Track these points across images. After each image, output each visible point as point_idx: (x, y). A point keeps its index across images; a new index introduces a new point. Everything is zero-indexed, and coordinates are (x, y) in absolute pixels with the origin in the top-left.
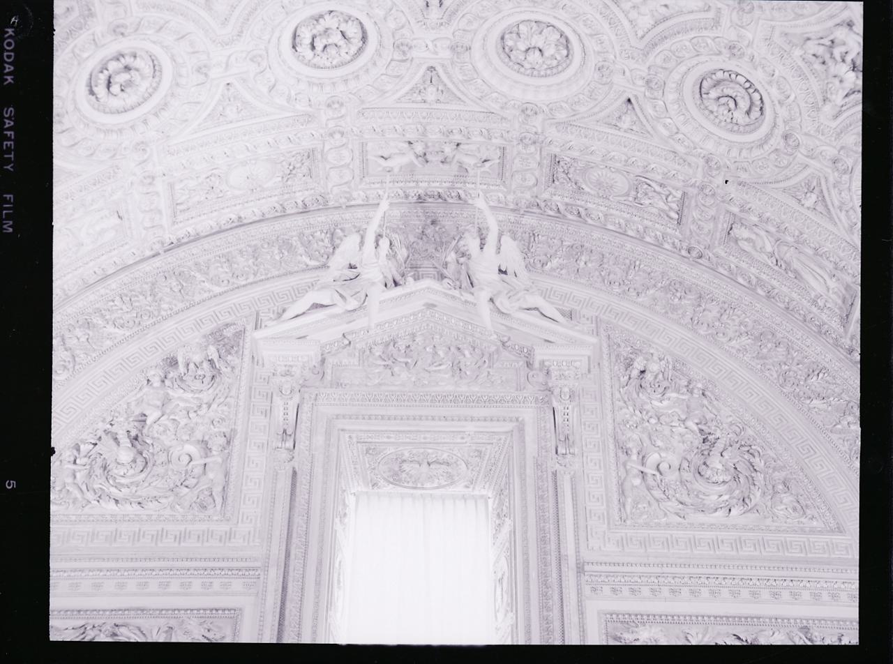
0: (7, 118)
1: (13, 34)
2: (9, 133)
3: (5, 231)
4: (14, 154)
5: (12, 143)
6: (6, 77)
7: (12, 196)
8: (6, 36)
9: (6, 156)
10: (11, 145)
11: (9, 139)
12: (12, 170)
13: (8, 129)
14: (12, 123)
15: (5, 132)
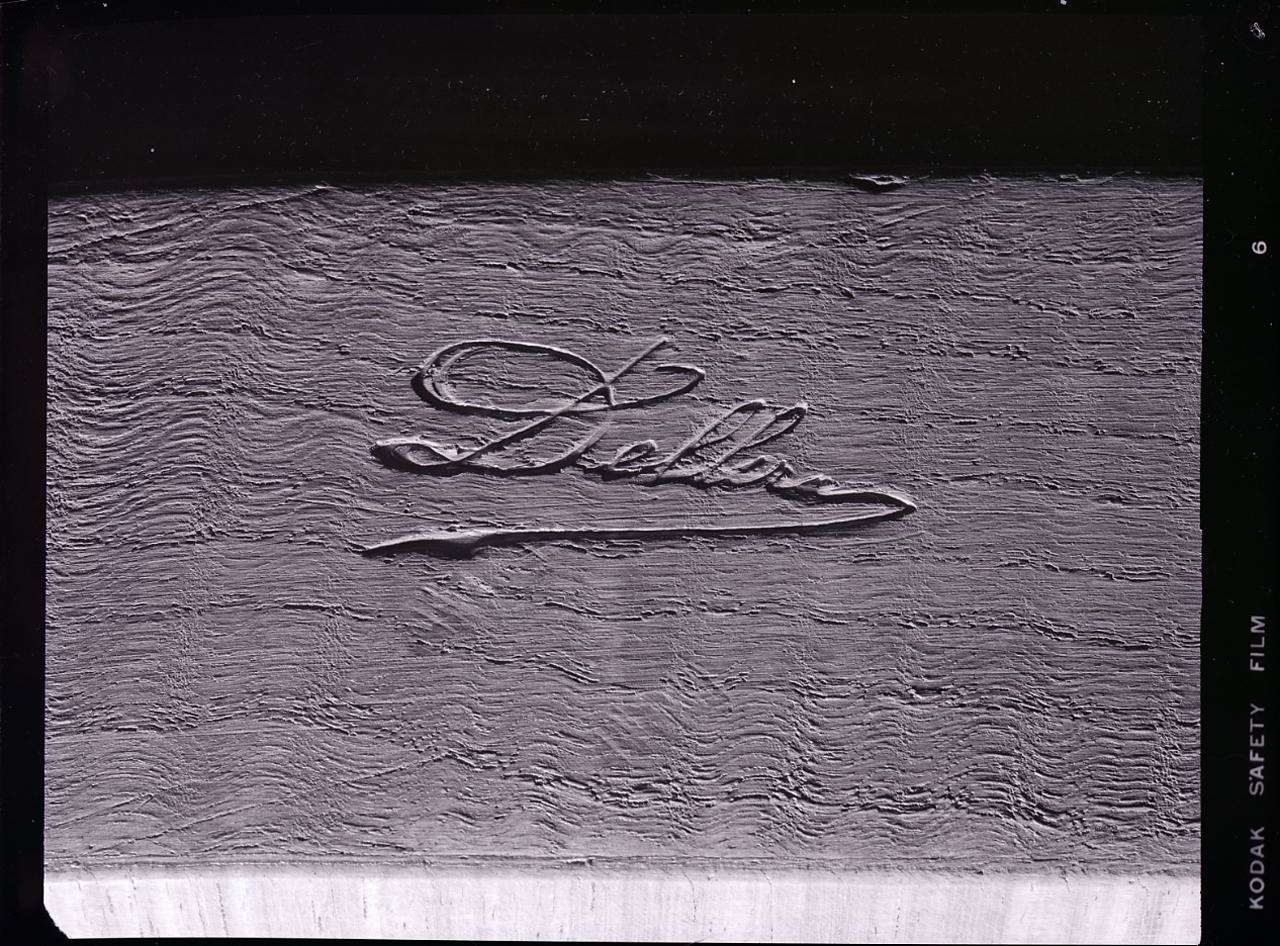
2: (1257, 758)
3: (1263, 618)
5: (1252, 744)
6: (1262, 838)
8: (1261, 898)
9: (1262, 726)
10: (1254, 742)
11: (1256, 750)
13: (1257, 764)
15: (1262, 759)
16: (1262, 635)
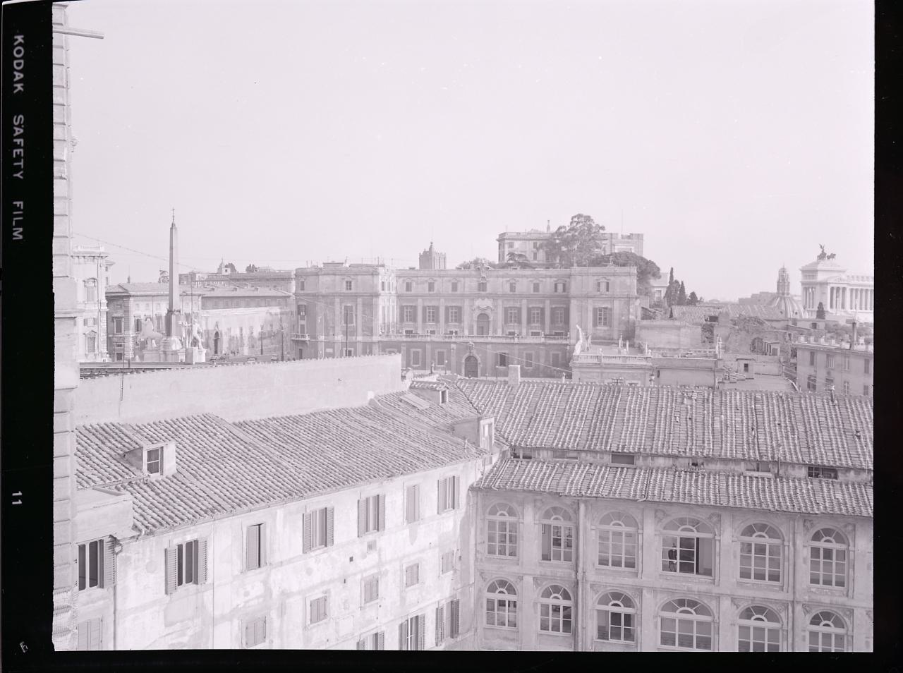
0: (18, 126)
1: (22, 41)
2: (18, 141)
3: (14, 239)
4: (24, 161)
5: (22, 150)
6: (15, 85)
7: (22, 203)
8: (16, 44)
9: (15, 164)
10: (20, 152)
11: (19, 147)
12: (21, 177)
13: (18, 137)
14: (22, 131)
15: (15, 140)
16: (15, 227)
